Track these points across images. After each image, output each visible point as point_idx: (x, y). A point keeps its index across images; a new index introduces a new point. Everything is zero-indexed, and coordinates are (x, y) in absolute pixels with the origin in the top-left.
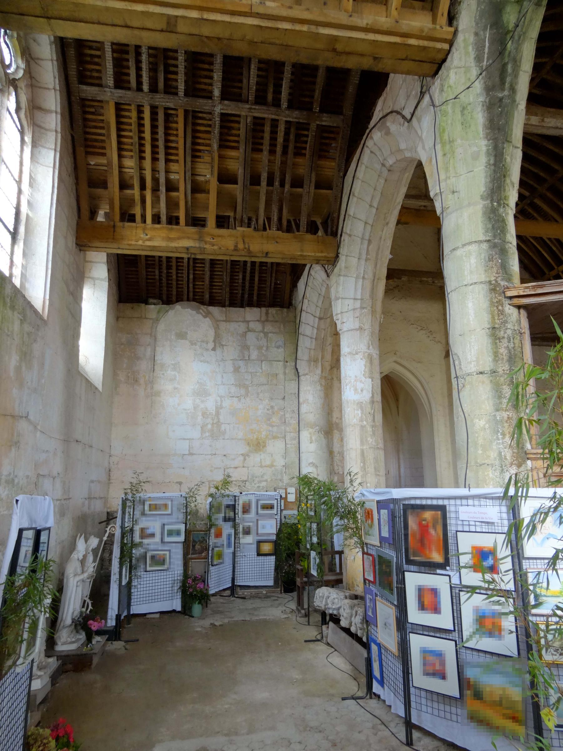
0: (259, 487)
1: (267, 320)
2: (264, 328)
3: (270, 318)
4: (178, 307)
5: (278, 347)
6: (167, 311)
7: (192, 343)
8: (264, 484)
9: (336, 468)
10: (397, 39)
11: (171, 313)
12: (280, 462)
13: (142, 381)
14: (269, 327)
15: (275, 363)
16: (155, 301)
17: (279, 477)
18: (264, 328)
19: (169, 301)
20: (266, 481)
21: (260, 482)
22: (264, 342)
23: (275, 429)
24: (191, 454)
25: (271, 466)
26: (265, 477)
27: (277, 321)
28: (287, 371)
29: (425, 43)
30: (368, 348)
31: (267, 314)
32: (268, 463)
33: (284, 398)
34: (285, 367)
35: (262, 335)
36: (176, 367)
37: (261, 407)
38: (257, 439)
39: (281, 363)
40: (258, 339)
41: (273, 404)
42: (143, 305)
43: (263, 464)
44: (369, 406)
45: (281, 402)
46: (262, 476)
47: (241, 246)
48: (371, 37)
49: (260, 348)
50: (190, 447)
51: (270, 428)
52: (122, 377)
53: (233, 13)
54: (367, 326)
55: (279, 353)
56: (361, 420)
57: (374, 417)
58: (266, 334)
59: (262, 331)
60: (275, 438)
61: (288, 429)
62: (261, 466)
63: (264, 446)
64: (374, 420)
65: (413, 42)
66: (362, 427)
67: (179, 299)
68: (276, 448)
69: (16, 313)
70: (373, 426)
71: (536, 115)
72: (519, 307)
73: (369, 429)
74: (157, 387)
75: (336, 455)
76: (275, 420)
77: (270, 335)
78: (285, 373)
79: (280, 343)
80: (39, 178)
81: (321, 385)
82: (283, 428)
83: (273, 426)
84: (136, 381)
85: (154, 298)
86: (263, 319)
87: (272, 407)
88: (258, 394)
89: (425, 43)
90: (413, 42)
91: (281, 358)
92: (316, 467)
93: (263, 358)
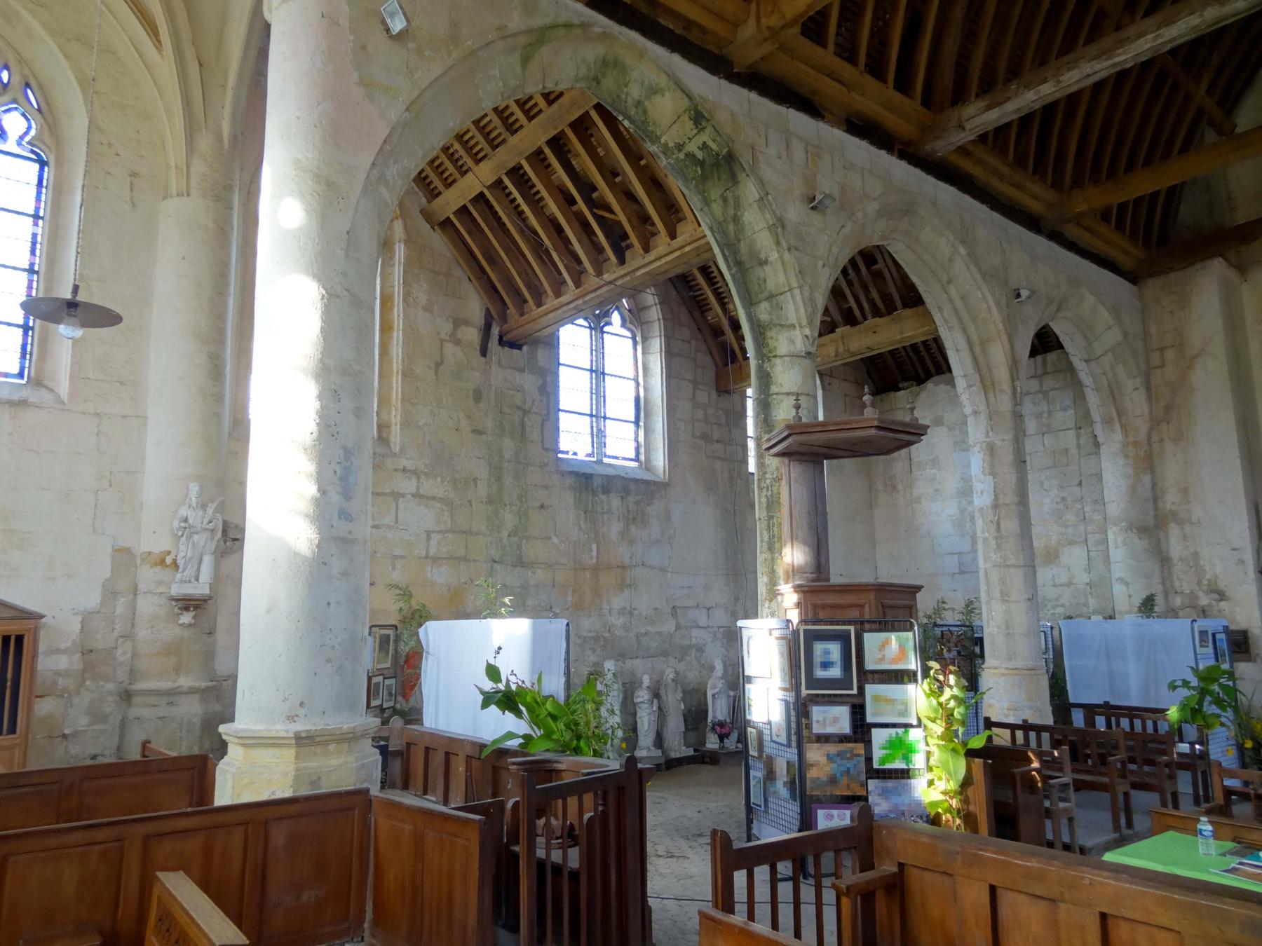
0: (1053, 614)
1: (1045, 373)
2: (1041, 385)
3: (1050, 368)
4: (929, 385)
5: (1065, 410)
6: (918, 394)
7: (950, 429)
8: (1060, 610)
9: (1177, 584)
10: (678, 253)
11: (923, 395)
12: (1083, 578)
13: (900, 487)
14: (1049, 382)
15: (1061, 434)
16: (905, 384)
17: (1082, 600)
18: (1041, 385)
19: (920, 381)
20: (1063, 606)
21: (1054, 607)
22: (1043, 406)
23: (1070, 530)
24: (962, 572)
25: (1069, 584)
26: (1062, 601)
27: (1060, 371)
28: (1082, 442)
29: (695, 245)
30: (987, 436)
31: (1044, 363)
32: (1064, 579)
33: (1080, 483)
34: (1078, 436)
35: (1040, 396)
36: (935, 462)
37: (1047, 500)
38: (1046, 547)
39: (1072, 432)
40: (1034, 403)
41: (1064, 494)
42: (892, 394)
43: (1057, 581)
44: (991, 512)
45: (1078, 489)
46: (1057, 599)
47: (841, 350)
48: (663, 261)
49: (1039, 416)
50: (961, 564)
51: (1063, 530)
52: (879, 486)
53: (595, 290)
54: (982, 407)
55: (1065, 417)
56: (983, 532)
57: (998, 524)
58: (1045, 394)
59: (1040, 392)
60: (1071, 543)
61: (1090, 529)
62: (1055, 585)
63: (1057, 556)
64: (998, 530)
65: (687, 249)
66: (985, 540)
67: (929, 376)
68: (1074, 558)
69: (613, 495)
70: (997, 538)
71: (1045, 81)
72: (776, 455)
73: (993, 542)
74: (916, 492)
75: (1175, 562)
76: (1070, 517)
77: (1052, 394)
78: (1079, 446)
79: (1069, 402)
80: (652, 365)
81: (1126, 456)
82: (1082, 528)
83: (1067, 527)
84: (894, 488)
85: (905, 380)
86: (1039, 373)
87: (1064, 499)
88: (1042, 483)
89: (695, 245)
90: (687, 249)
91: (1071, 425)
92: (1127, 584)
93: (1044, 430)
